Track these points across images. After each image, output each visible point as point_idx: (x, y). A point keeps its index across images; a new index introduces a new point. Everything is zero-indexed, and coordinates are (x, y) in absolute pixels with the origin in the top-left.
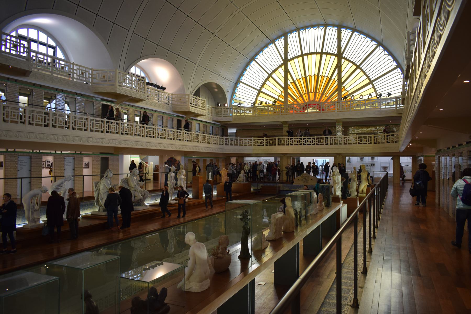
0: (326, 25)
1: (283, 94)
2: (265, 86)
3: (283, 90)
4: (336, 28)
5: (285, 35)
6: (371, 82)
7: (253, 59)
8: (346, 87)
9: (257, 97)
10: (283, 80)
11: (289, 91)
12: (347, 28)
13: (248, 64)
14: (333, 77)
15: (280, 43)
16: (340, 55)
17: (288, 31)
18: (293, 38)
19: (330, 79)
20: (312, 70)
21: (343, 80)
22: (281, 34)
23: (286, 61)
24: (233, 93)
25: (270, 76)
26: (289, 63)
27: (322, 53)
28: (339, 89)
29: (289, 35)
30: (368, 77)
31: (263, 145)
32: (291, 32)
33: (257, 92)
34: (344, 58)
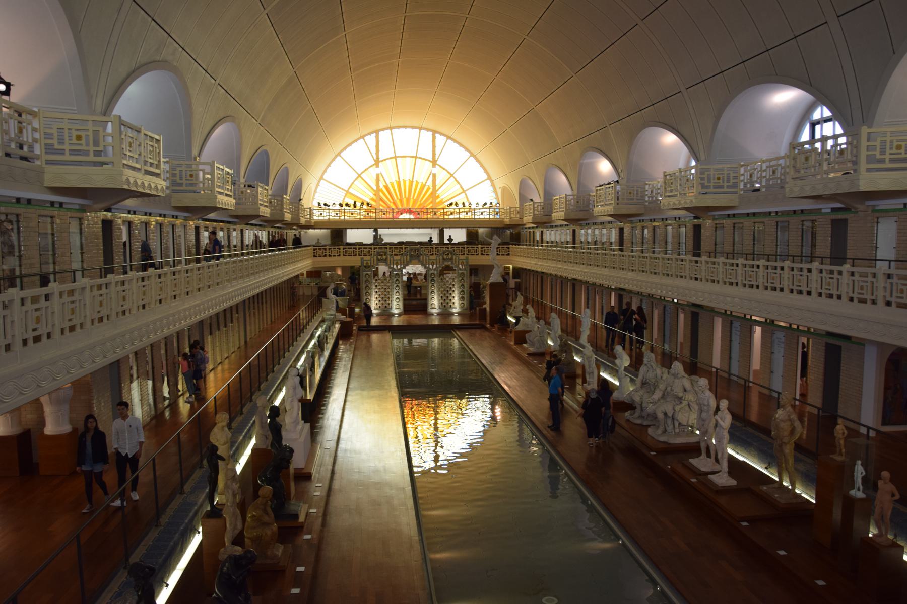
0: (421, 129)
1: (375, 197)
2: (353, 185)
3: (374, 193)
4: (430, 134)
5: (377, 132)
6: (464, 191)
7: (339, 154)
8: (440, 195)
9: (344, 198)
10: (375, 182)
11: (381, 194)
12: (441, 134)
13: (334, 159)
14: (427, 184)
15: (371, 139)
16: (434, 162)
17: (378, 127)
18: (384, 136)
19: (425, 185)
20: (406, 175)
21: (437, 188)
22: (370, 131)
23: (377, 162)
24: (315, 192)
25: (359, 176)
26: (380, 163)
27: (416, 157)
28: (434, 195)
29: (381, 133)
30: (461, 187)
31: (356, 255)
32: (383, 130)
33: (345, 192)
34: (438, 165)
